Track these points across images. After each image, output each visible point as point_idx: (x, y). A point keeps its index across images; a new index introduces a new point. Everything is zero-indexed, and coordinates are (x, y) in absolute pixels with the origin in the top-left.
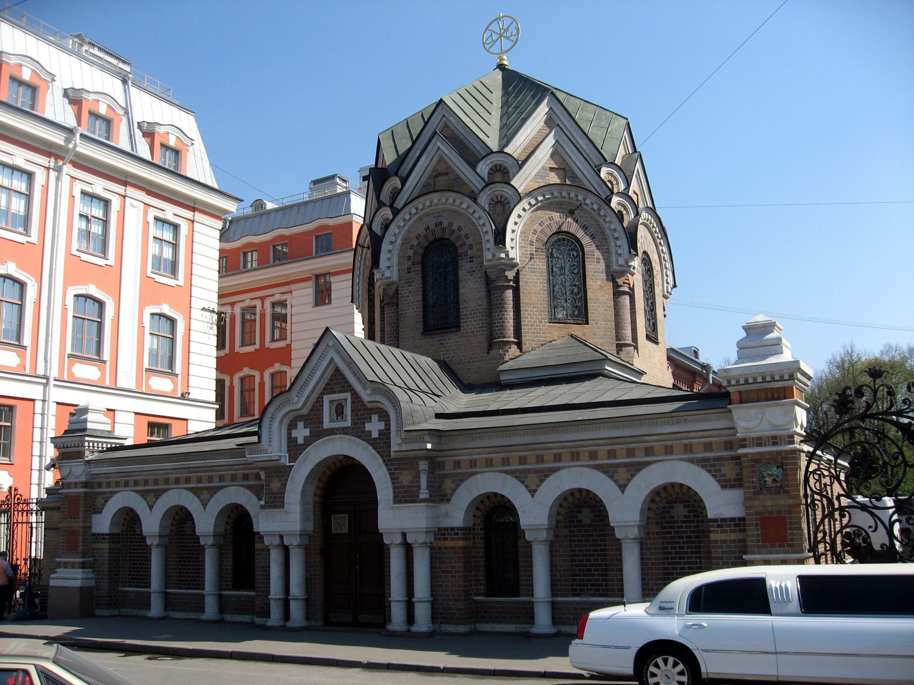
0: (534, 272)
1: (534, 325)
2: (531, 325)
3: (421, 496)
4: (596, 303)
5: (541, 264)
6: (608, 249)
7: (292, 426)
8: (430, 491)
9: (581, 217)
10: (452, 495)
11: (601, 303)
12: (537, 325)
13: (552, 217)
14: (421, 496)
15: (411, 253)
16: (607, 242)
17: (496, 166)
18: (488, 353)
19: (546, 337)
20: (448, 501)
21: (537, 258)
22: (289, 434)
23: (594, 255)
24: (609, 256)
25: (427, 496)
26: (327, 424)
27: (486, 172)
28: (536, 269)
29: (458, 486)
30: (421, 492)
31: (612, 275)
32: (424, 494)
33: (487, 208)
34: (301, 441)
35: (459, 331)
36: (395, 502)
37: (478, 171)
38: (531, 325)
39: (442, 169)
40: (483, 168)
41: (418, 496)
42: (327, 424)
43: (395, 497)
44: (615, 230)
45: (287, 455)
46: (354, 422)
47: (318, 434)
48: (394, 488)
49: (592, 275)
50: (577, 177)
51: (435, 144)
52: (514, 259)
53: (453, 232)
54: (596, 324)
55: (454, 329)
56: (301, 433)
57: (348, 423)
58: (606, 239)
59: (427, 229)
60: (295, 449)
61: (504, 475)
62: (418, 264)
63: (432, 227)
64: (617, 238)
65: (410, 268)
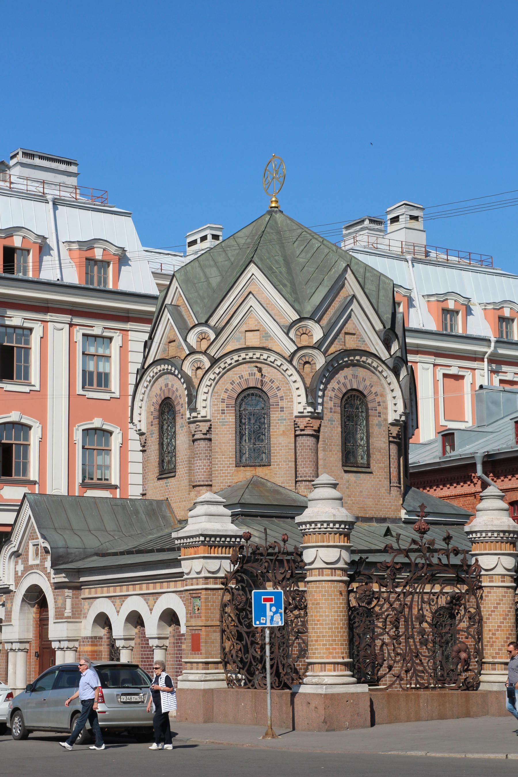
0: (224, 425)
1: (222, 470)
2: (221, 470)
3: (66, 615)
4: (278, 447)
5: (231, 418)
6: (292, 398)
7: (16, 563)
8: (72, 611)
9: (268, 373)
10: (87, 613)
11: (283, 446)
12: (225, 470)
13: (242, 376)
14: (66, 615)
15: (152, 409)
16: (291, 392)
17: (201, 333)
18: (189, 494)
19: (233, 479)
20: (86, 617)
21: (227, 413)
22: (15, 568)
23: (278, 405)
24: (293, 405)
25: (70, 615)
26: (31, 562)
27: (195, 341)
28: (227, 422)
29: (90, 607)
30: (66, 611)
31: (295, 421)
32: (68, 612)
33: (189, 373)
34: (20, 574)
35: (174, 476)
36: (57, 618)
37: (188, 340)
38: (221, 470)
39: (172, 338)
40: (192, 338)
41: (63, 615)
42: (31, 562)
43: (56, 615)
44: (295, 382)
45: (14, 584)
46: (41, 562)
47: (28, 568)
48: (56, 608)
49: (277, 423)
50: (270, 336)
51: (166, 316)
52: (206, 417)
53: (173, 392)
54: (278, 465)
55: (172, 474)
56: (20, 568)
57: (38, 562)
58: (290, 390)
59: (161, 389)
60: (18, 580)
61: (107, 599)
62: (156, 419)
63: (163, 388)
64: (298, 389)
65: (152, 422)
